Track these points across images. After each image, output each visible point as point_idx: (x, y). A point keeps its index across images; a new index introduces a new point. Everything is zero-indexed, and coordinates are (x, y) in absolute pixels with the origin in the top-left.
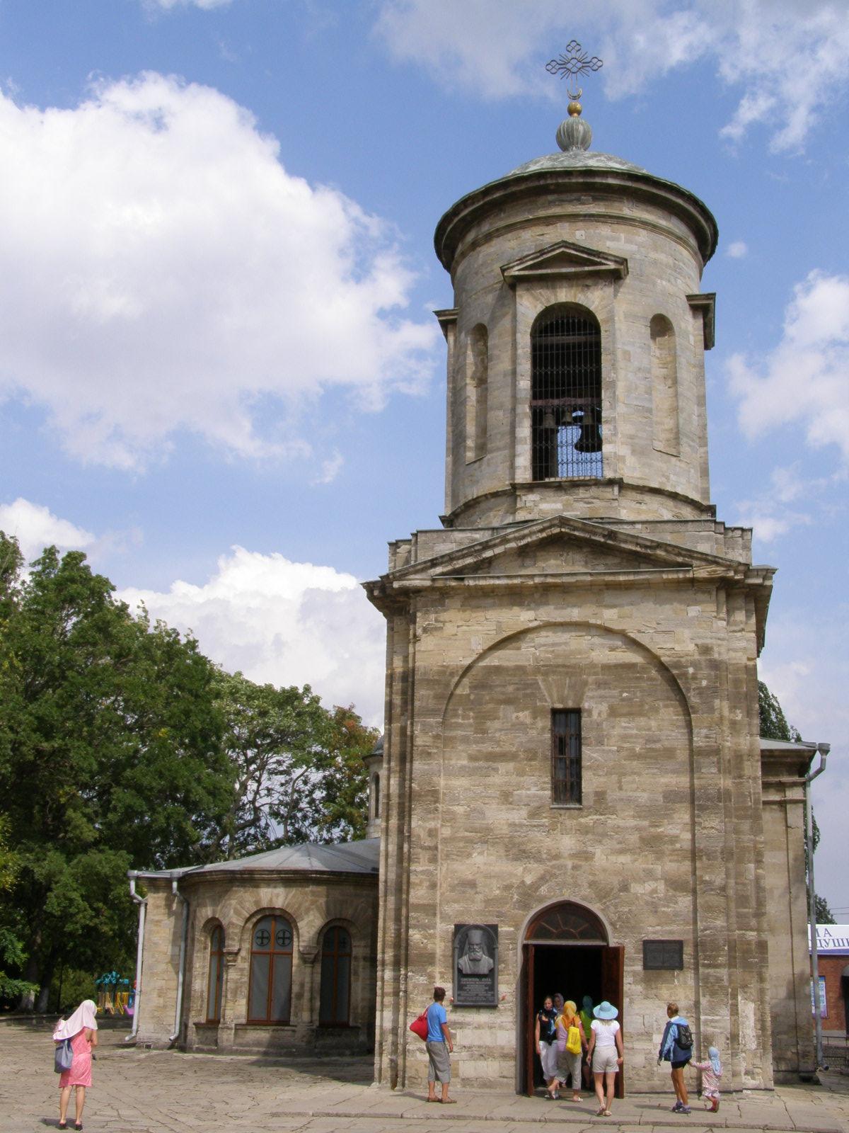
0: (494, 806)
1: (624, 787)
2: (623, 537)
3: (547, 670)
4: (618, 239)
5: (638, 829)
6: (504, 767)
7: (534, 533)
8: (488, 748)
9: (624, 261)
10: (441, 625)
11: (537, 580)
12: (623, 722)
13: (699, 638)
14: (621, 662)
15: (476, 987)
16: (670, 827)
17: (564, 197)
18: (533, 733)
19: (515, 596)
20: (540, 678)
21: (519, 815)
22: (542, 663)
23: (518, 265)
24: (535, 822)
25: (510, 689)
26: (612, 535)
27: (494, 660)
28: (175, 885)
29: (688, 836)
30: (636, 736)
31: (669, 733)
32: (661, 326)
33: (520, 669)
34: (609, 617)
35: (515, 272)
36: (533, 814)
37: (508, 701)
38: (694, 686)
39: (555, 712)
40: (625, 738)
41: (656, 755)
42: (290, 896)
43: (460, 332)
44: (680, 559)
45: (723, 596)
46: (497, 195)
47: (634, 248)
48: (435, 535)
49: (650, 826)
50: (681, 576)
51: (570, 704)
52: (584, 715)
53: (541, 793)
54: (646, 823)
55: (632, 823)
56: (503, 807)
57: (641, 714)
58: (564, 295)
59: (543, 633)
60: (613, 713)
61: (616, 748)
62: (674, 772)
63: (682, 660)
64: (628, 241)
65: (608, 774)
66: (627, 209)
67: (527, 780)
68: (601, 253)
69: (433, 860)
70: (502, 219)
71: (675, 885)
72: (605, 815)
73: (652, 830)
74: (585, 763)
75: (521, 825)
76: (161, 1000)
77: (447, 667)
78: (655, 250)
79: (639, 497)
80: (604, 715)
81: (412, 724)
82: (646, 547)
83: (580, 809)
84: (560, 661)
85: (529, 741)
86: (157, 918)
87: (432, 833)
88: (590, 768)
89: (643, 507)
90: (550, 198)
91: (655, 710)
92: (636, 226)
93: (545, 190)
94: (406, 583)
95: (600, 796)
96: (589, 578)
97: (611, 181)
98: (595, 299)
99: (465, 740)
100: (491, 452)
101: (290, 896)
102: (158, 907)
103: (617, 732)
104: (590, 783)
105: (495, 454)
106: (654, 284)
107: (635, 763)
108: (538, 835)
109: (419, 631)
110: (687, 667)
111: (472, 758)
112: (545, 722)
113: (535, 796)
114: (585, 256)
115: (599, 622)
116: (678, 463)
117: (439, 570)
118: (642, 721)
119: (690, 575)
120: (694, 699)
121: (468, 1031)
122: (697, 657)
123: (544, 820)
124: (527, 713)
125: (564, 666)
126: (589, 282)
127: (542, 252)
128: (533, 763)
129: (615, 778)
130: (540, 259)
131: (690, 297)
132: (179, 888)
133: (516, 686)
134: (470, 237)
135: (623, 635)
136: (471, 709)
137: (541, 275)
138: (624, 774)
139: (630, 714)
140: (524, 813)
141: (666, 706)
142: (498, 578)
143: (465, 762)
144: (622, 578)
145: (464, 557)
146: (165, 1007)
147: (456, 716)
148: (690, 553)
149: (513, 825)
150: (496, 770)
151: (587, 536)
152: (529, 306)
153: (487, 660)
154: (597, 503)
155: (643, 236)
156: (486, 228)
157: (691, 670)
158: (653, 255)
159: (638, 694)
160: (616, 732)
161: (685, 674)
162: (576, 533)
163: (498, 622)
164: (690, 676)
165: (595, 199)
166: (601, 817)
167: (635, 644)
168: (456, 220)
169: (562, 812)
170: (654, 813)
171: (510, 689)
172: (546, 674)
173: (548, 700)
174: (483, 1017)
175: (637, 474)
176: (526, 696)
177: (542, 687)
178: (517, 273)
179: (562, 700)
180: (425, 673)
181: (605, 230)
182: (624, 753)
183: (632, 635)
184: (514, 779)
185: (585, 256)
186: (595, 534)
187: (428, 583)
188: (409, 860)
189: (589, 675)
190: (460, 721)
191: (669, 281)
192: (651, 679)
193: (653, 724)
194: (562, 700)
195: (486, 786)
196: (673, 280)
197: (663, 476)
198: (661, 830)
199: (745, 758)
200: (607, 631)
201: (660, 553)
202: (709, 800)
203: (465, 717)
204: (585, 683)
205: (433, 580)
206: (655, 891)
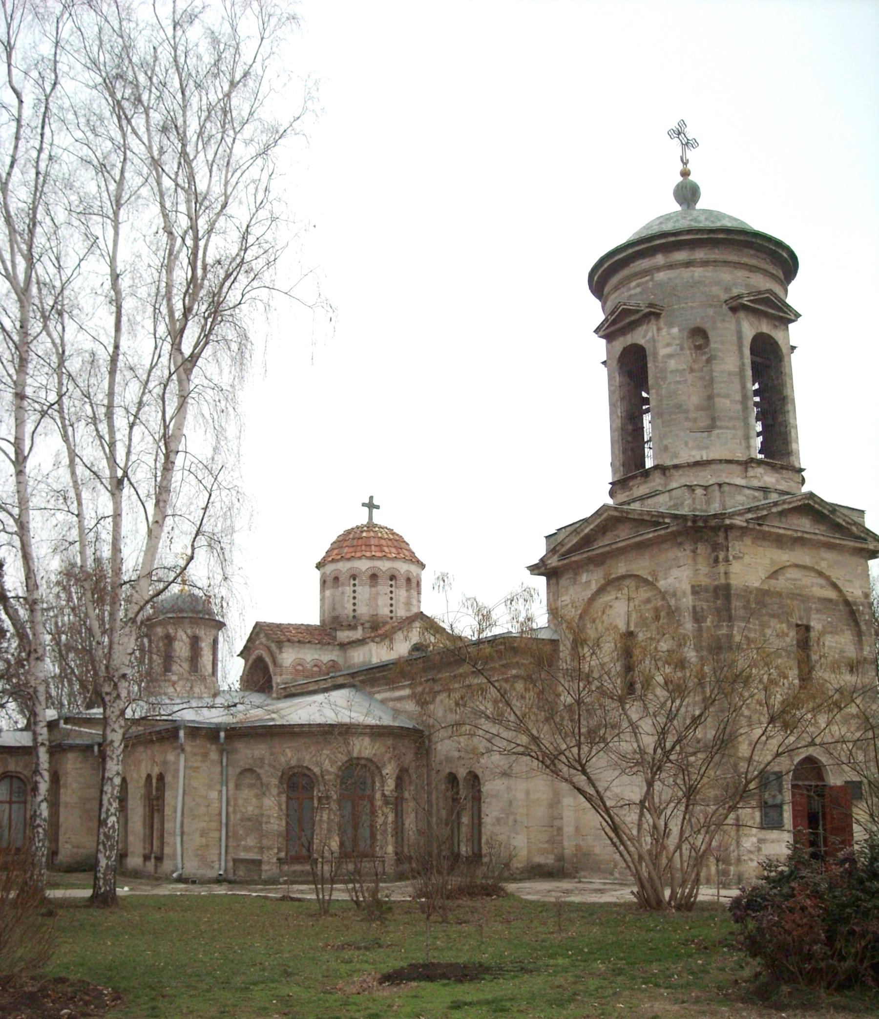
2: (838, 514)
3: (793, 596)
9: (798, 315)
10: (741, 555)
11: (799, 534)
15: (773, 814)
17: (759, 254)
18: (788, 640)
19: (779, 541)
28: (222, 734)
30: (836, 648)
34: (823, 566)
35: (745, 301)
37: (773, 616)
39: (798, 625)
42: (376, 747)
43: (671, 325)
48: (734, 488)
51: (805, 622)
58: (765, 328)
59: (790, 570)
70: (714, 254)
76: (204, 840)
77: (747, 587)
82: (848, 523)
84: (797, 591)
86: (196, 765)
90: (752, 252)
93: (749, 245)
94: (734, 521)
96: (822, 538)
100: (721, 428)
101: (376, 747)
102: (195, 754)
109: (731, 558)
115: (819, 568)
117: (750, 516)
119: (866, 546)
120: (864, 628)
121: (768, 845)
122: (863, 600)
125: (800, 595)
126: (777, 324)
127: (760, 293)
132: (226, 737)
134: (681, 256)
135: (828, 578)
139: (831, 633)
142: (780, 528)
144: (838, 541)
145: (763, 509)
146: (207, 846)
151: (820, 508)
152: (749, 329)
156: (700, 254)
157: (861, 608)
161: (859, 610)
162: (816, 506)
165: (773, 263)
167: (835, 586)
168: (673, 239)
174: (774, 835)
179: (801, 619)
180: (736, 590)
183: (835, 580)
186: (824, 508)
187: (745, 524)
192: (840, 610)
194: (801, 619)
200: (820, 574)
201: (854, 529)
203: (755, 625)
205: (747, 521)
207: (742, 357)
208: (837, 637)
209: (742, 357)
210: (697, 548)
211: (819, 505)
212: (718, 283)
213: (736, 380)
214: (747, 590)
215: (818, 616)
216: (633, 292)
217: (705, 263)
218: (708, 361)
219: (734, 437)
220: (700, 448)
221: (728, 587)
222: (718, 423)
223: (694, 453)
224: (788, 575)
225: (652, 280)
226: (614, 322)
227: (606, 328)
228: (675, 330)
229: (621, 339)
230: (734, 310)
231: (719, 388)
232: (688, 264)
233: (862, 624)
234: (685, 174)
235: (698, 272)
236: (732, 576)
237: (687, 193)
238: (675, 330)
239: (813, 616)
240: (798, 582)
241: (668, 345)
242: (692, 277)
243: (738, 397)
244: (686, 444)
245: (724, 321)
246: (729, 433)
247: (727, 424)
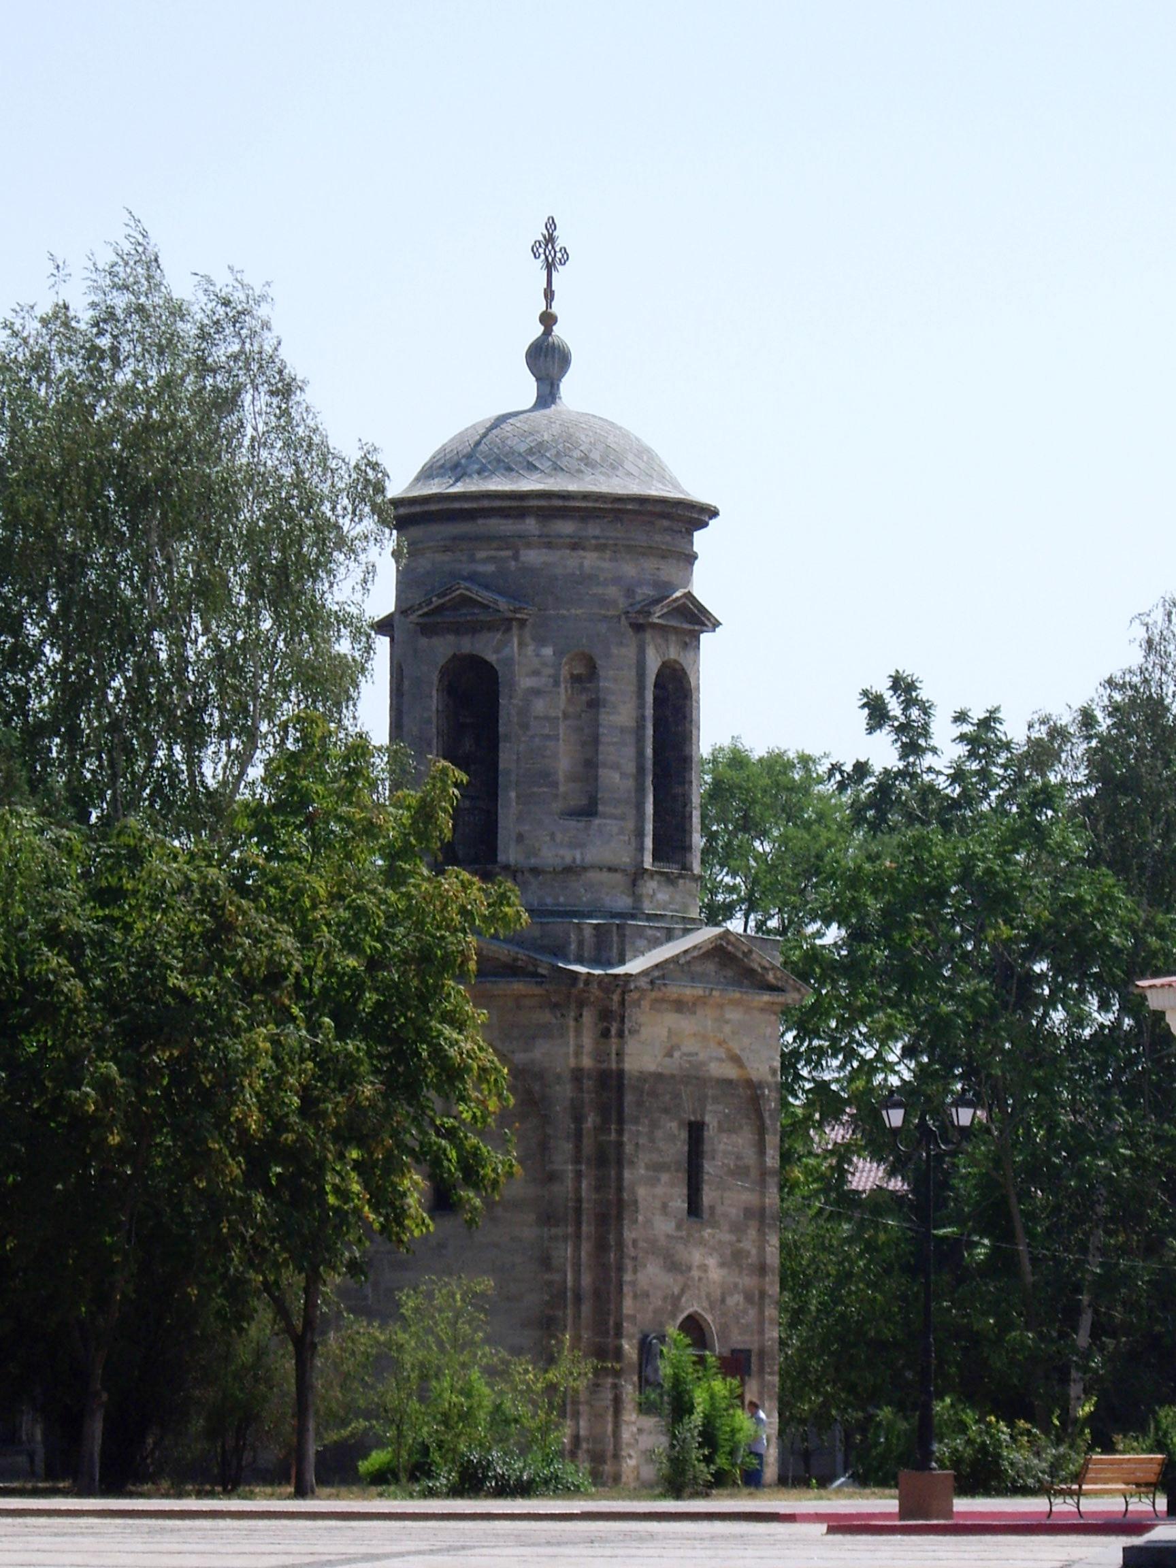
5: (731, 1244)
6: (665, 1177)
9: (716, 624)
24: (679, 1234)
29: (754, 1251)
33: (673, 1076)
36: (679, 1227)
37: (666, 1111)
41: (740, 1172)
43: (541, 641)
46: (630, 507)
51: (699, 1118)
60: (721, 1129)
69: (635, 1271)
71: (749, 1298)
74: (706, 1177)
81: (620, 1132)
87: (635, 1242)
95: (712, 1208)
100: (604, 816)
103: (722, 1147)
104: (708, 1196)
105: (608, 821)
108: (680, 1247)
109: (626, 1032)
111: (647, 1167)
112: (684, 1135)
134: (566, 527)
140: (673, 1224)
149: (668, 1236)
150: (659, 1180)
156: (593, 529)
157: (767, 1092)
160: (722, 1147)
161: (763, 1094)
162: (730, 948)
168: (560, 503)
171: (668, 1097)
178: (657, 621)
179: (694, 1112)
188: (620, 1269)
194: (694, 1112)
195: (654, 1197)
206: (738, 1304)
207: (641, 706)
208: (734, 1136)
209: (641, 706)
210: (581, 1015)
211: (733, 945)
212: (617, 580)
213: (630, 739)
214: (643, 1077)
216: (481, 568)
217: (600, 548)
218: (594, 704)
219: (621, 831)
220: (573, 845)
221: (621, 1073)
222: (601, 808)
223: (562, 852)
225: (516, 557)
226: (440, 609)
227: (425, 614)
228: (548, 651)
229: (451, 638)
230: (638, 628)
231: (608, 752)
232: (576, 545)
233: (766, 1115)
234: (548, 320)
235: (590, 560)
236: (627, 1059)
237: (548, 360)
238: (548, 651)
239: (709, 1108)
241: (536, 673)
242: (581, 565)
243: (631, 768)
244: (553, 836)
245: (621, 644)
246: (612, 826)
247: (614, 811)
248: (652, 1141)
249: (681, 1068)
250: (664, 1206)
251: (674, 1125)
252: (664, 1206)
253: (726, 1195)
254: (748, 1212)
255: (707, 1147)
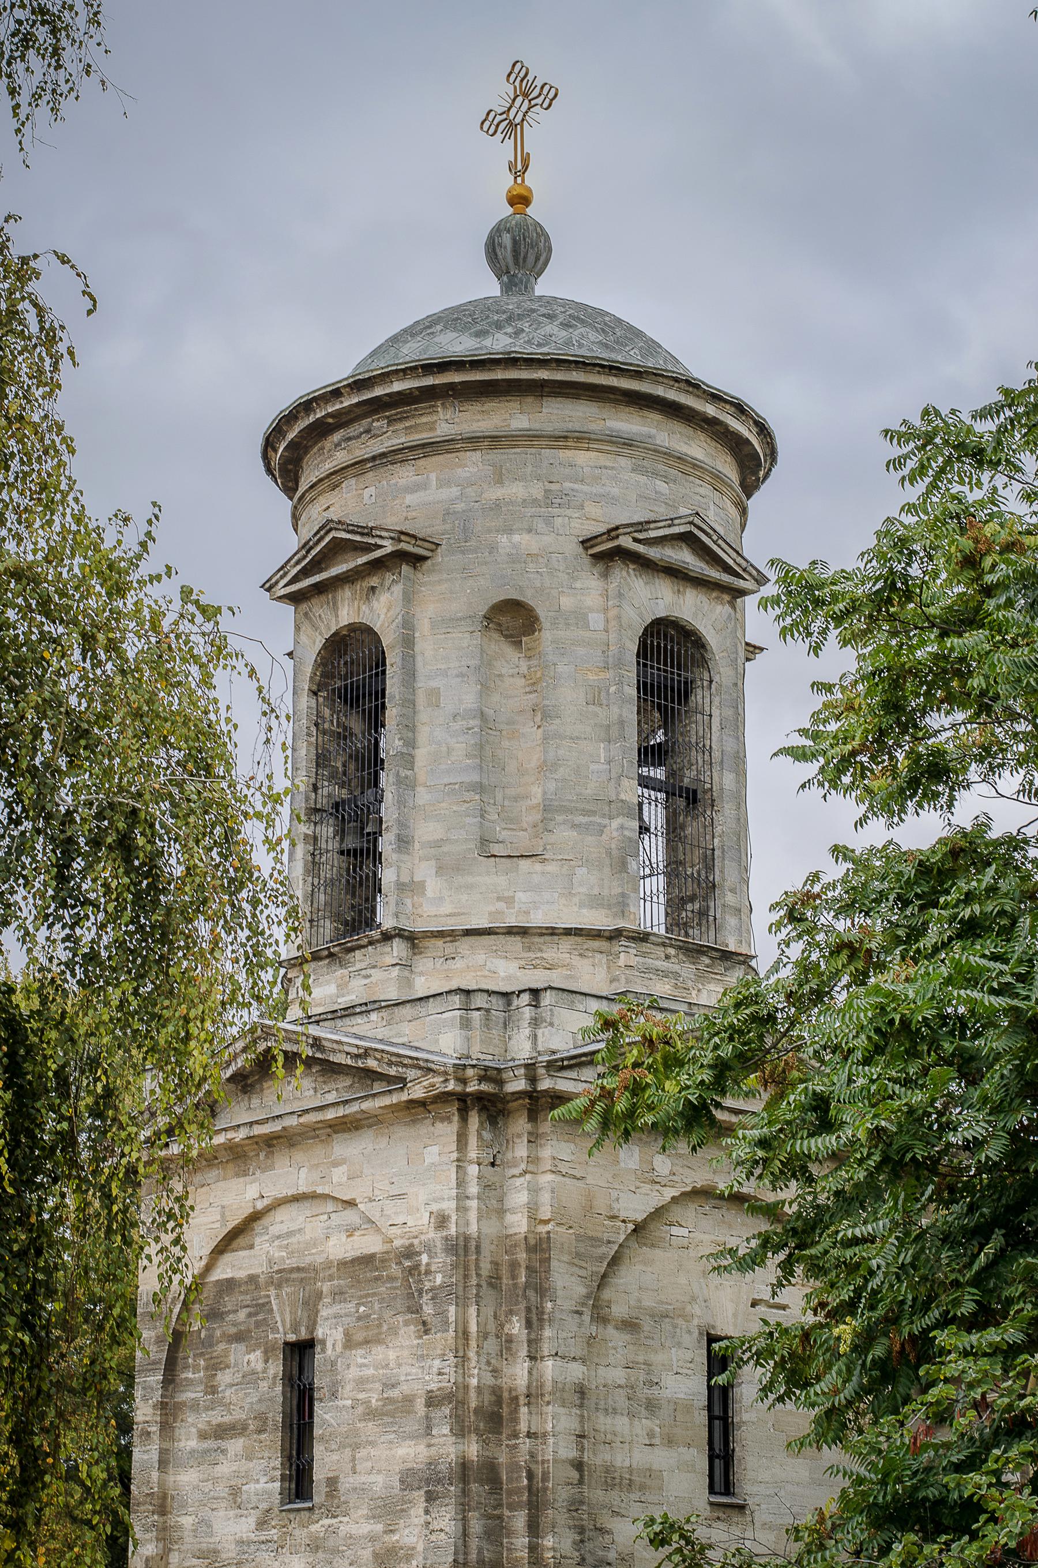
0: (222, 1513)
1: (358, 1468)
3: (282, 1277)
4: (423, 486)
5: (372, 1538)
7: (236, 1056)
8: (217, 1417)
12: (358, 1356)
13: (435, 1200)
14: (358, 1254)
16: (407, 1531)
20: (272, 1292)
21: (245, 1526)
22: (276, 1268)
23: (282, 577)
25: (242, 1315)
26: (317, 1043)
27: (225, 1270)
31: (408, 1369)
32: (513, 619)
33: (252, 1279)
36: (262, 1524)
37: (239, 1337)
38: (427, 1285)
40: (361, 1383)
44: (392, 1071)
45: (474, 1120)
47: (455, 491)
49: (385, 1532)
50: (395, 1099)
51: (304, 1335)
52: (318, 1349)
53: (270, 1485)
54: (379, 1527)
55: (365, 1528)
56: (232, 1513)
57: (378, 1341)
60: (349, 1343)
61: (350, 1402)
62: (412, 1437)
63: (416, 1242)
64: (442, 484)
65: (342, 1446)
66: (446, 421)
67: (256, 1466)
68: (372, 528)
72: (335, 1517)
73: (386, 1538)
74: (317, 1432)
75: (249, 1543)
78: (499, 481)
79: (450, 948)
80: (339, 1348)
82: (357, 1056)
83: (310, 1509)
85: (260, 1401)
88: (322, 1438)
89: (458, 964)
90: (336, 437)
91: (394, 1331)
92: (458, 451)
95: (332, 1482)
97: (397, 386)
98: (380, 610)
99: (195, 1406)
103: (353, 1373)
106: (493, 548)
107: (370, 1424)
110: (419, 1254)
111: (203, 1436)
112: (276, 1368)
113: (265, 1492)
114: (358, 538)
116: (538, 867)
118: (379, 1352)
119: (404, 1097)
122: (431, 1235)
123: (274, 1531)
124: (258, 1353)
125: (298, 1269)
126: (374, 581)
128: (263, 1436)
129: (348, 1452)
130: (308, 560)
131: (586, 543)
133: (248, 1310)
136: (202, 1354)
137: (315, 586)
138: (356, 1447)
140: (252, 1521)
141: (406, 1323)
143: (193, 1443)
147: (186, 1367)
148: (397, 1060)
149: (241, 1542)
150: (224, 1452)
153: (219, 1270)
154: (377, 975)
155: (472, 465)
157: (424, 1258)
158: (496, 493)
159: (377, 1306)
160: (353, 1373)
163: (223, 1207)
164: (423, 1268)
166: (334, 1521)
169: (292, 1516)
170: (390, 1511)
171: (242, 1315)
172: (279, 1286)
173: (281, 1329)
175: (447, 908)
176: (258, 1324)
177: (275, 1307)
181: (404, 475)
182: (360, 1409)
184: (244, 1466)
185: (358, 538)
189: (323, 1280)
190: (190, 1375)
191: (530, 531)
193: (392, 1355)
195: (215, 1480)
196: (541, 526)
197: (499, 899)
198: (396, 1537)
199: (522, 1400)
202: (439, 1481)
204: (319, 1295)
215: (336, 1308)
224: (275, 1230)
239: (324, 1313)
240: (293, 1240)
248: (212, 1390)
249: (270, 1262)
250: (235, 1492)
251: (255, 1358)
252: (235, 1492)
253: (362, 1453)
254: (409, 1480)
255: (320, 1381)
